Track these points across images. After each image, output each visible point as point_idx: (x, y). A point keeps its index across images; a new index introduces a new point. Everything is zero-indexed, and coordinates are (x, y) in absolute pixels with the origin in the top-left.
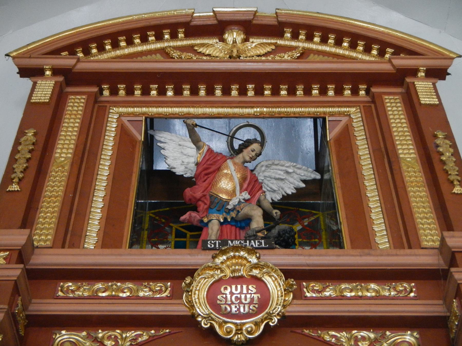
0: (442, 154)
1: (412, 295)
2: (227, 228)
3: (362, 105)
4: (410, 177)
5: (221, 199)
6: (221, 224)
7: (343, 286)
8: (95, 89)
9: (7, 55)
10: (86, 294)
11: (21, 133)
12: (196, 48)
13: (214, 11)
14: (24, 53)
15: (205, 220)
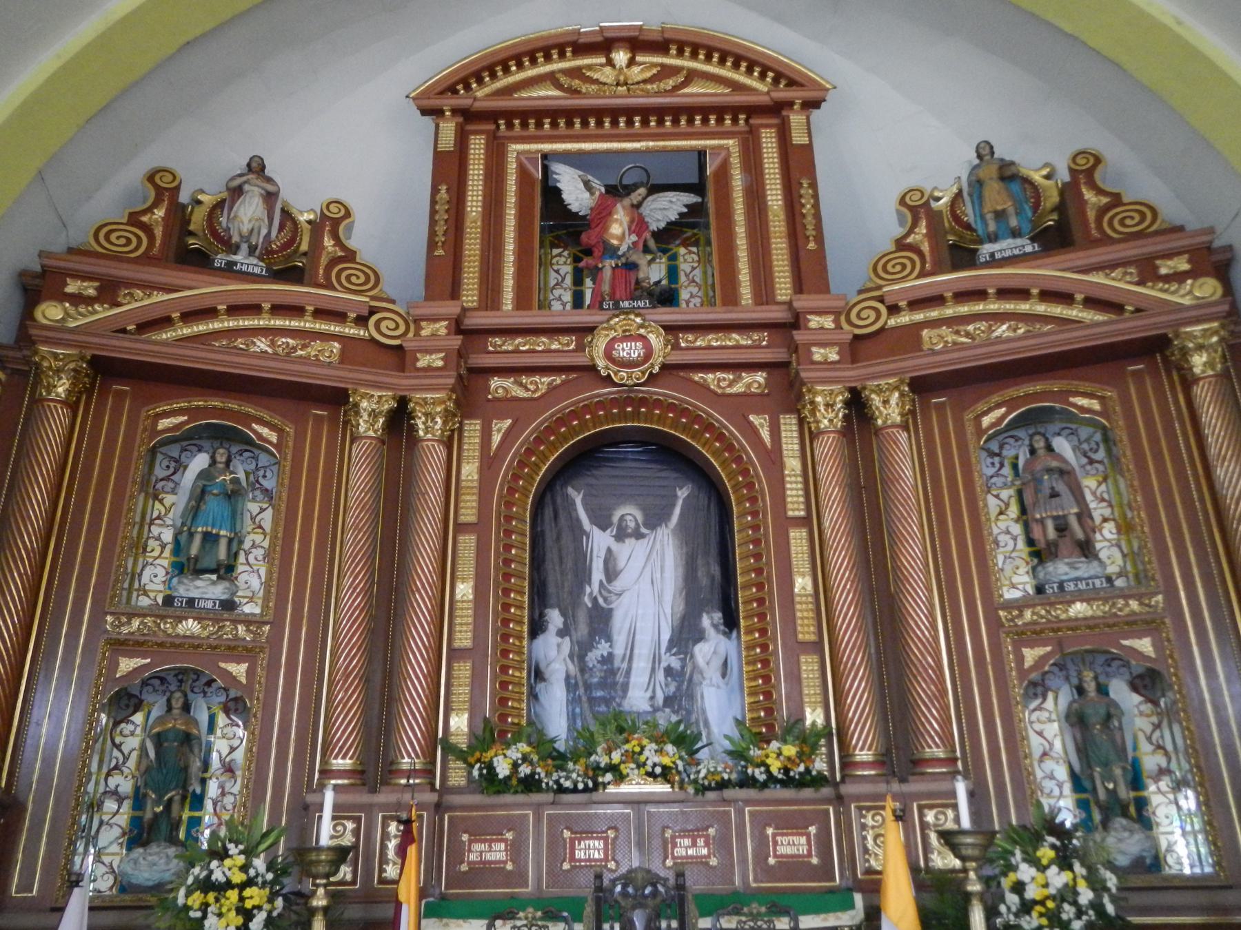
0: (803, 206)
1: (764, 343)
2: (618, 271)
3: (740, 136)
4: (775, 227)
5: (612, 245)
6: (613, 268)
7: (710, 337)
8: (493, 127)
9: (407, 97)
10: (510, 348)
11: (435, 190)
12: (584, 71)
13: (601, 27)
14: (423, 93)
15: (600, 266)
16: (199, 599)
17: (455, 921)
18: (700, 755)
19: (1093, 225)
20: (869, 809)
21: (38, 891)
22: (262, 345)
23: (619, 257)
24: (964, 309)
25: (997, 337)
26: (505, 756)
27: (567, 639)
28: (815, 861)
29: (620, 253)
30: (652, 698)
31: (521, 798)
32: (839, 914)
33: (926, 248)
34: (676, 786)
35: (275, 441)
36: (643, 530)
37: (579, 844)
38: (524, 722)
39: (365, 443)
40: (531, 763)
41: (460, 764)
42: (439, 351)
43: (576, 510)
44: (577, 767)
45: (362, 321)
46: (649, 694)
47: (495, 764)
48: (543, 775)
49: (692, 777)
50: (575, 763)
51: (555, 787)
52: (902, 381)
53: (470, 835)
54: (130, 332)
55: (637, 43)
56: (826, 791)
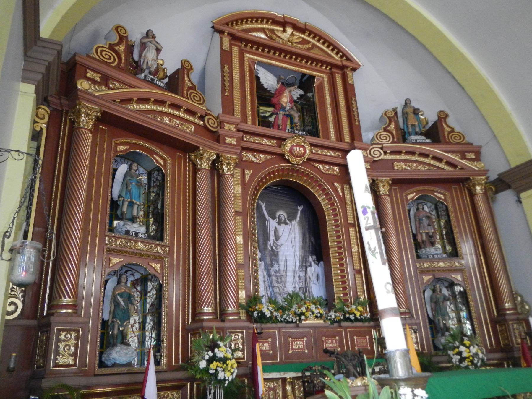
9: (212, 22)
12: (275, 31)
13: (283, 15)
16: (139, 233)
17: (266, 373)
19: (447, 137)
21: (88, 367)
22: (167, 120)
23: (286, 111)
24: (408, 157)
25: (419, 170)
27: (263, 262)
28: (369, 348)
29: (286, 110)
30: (295, 287)
31: (274, 325)
33: (394, 132)
35: (163, 164)
36: (287, 221)
39: (203, 172)
42: (234, 138)
43: (262, 210)
45: (202, 118)
52: (390, 179)
54: (117, 102)
55: (296, 27)
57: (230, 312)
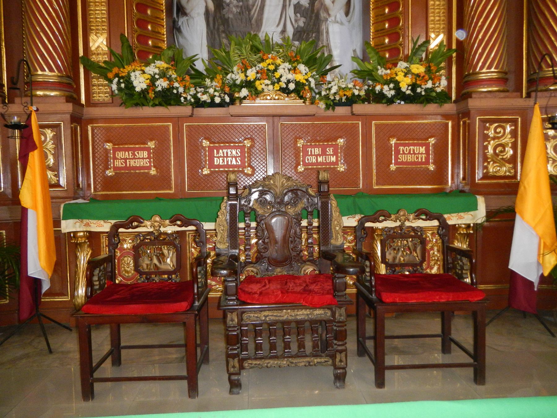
17: (95, 221)
18: (329, 78)
20: (492, 121)
26: (144, 72)
28: (432, 167)
30: (284, 31)
31: (161, 111)
32: (462, 214)
34: (308, 103)
37: (218, 153)
38: (164, 46)
40: (170, 79)
41: (102, 81)
44: (214, 83)
46: (280, 28)
47: (133, 78)
48: (181, 90)
49: (323, 93)
50: (212, 80)
51: (193, 100)
53: (114, 145)
56: (449, 108)
57: (40, 79)
